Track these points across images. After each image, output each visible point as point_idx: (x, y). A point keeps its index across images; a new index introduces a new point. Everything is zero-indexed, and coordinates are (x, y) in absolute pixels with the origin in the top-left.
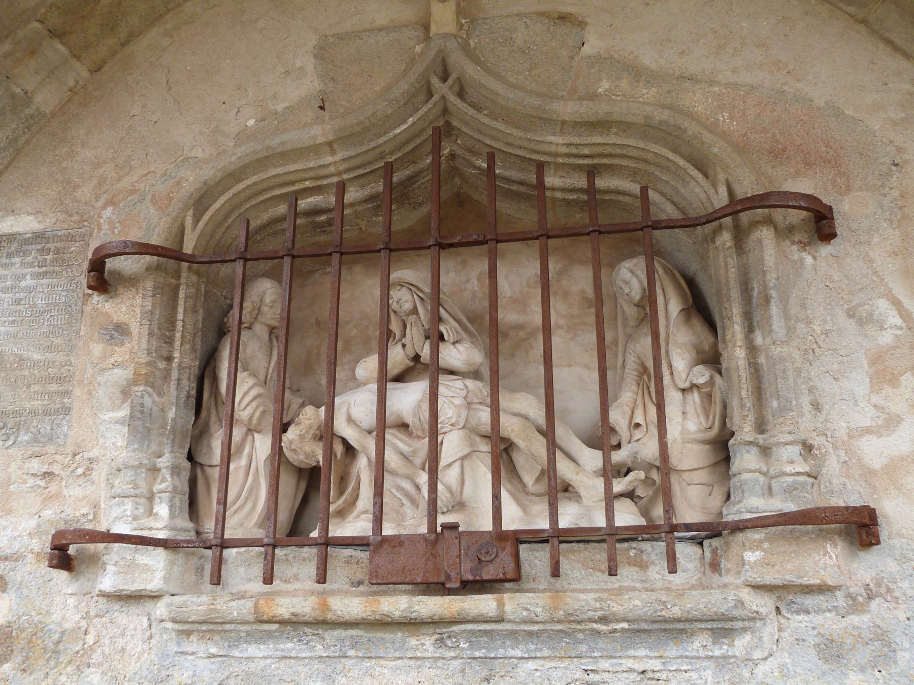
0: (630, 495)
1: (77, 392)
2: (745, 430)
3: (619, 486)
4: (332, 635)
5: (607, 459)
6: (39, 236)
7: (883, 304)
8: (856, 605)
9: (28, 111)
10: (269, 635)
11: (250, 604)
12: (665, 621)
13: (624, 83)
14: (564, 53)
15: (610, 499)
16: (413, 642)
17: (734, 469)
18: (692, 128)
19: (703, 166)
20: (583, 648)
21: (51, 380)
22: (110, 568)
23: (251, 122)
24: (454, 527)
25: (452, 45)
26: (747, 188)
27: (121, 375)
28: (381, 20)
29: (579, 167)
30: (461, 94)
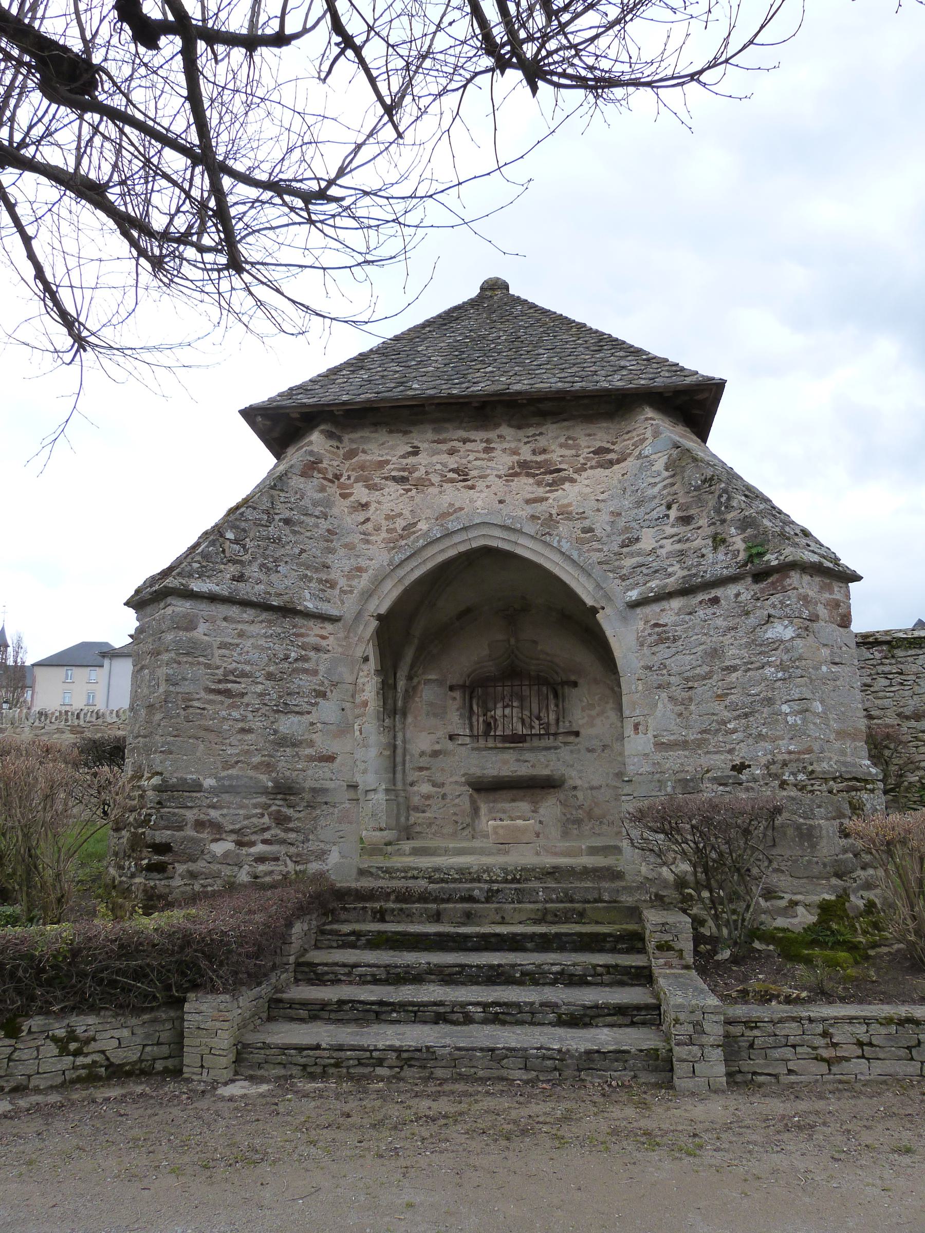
2: (561, 719)
6: (436, 680)
8: (576, 745)
19: (557, 673)
26: (564, 679)
27: (456, 707)
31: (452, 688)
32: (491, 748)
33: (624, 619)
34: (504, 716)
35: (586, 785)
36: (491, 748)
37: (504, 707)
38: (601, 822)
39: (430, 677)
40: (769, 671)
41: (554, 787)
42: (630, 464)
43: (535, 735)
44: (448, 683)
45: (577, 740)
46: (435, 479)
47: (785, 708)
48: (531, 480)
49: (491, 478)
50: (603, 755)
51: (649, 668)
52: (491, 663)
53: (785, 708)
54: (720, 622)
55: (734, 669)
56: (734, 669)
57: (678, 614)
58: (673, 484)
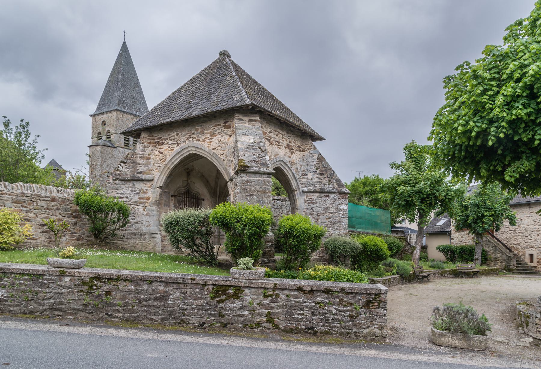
31: (172, 196)
33: (301, 195)
40: (340, 215)
42: (306, 153)
46: (274, 143)
47: (343, 224)
48: (289, 150)
49: (283, 147)
51: (308, 209)
53: (343, 224)
54: (329, 202)
55: (331, 213)
56: (331, 213)
57: (317, 197)
58: (318, 164)
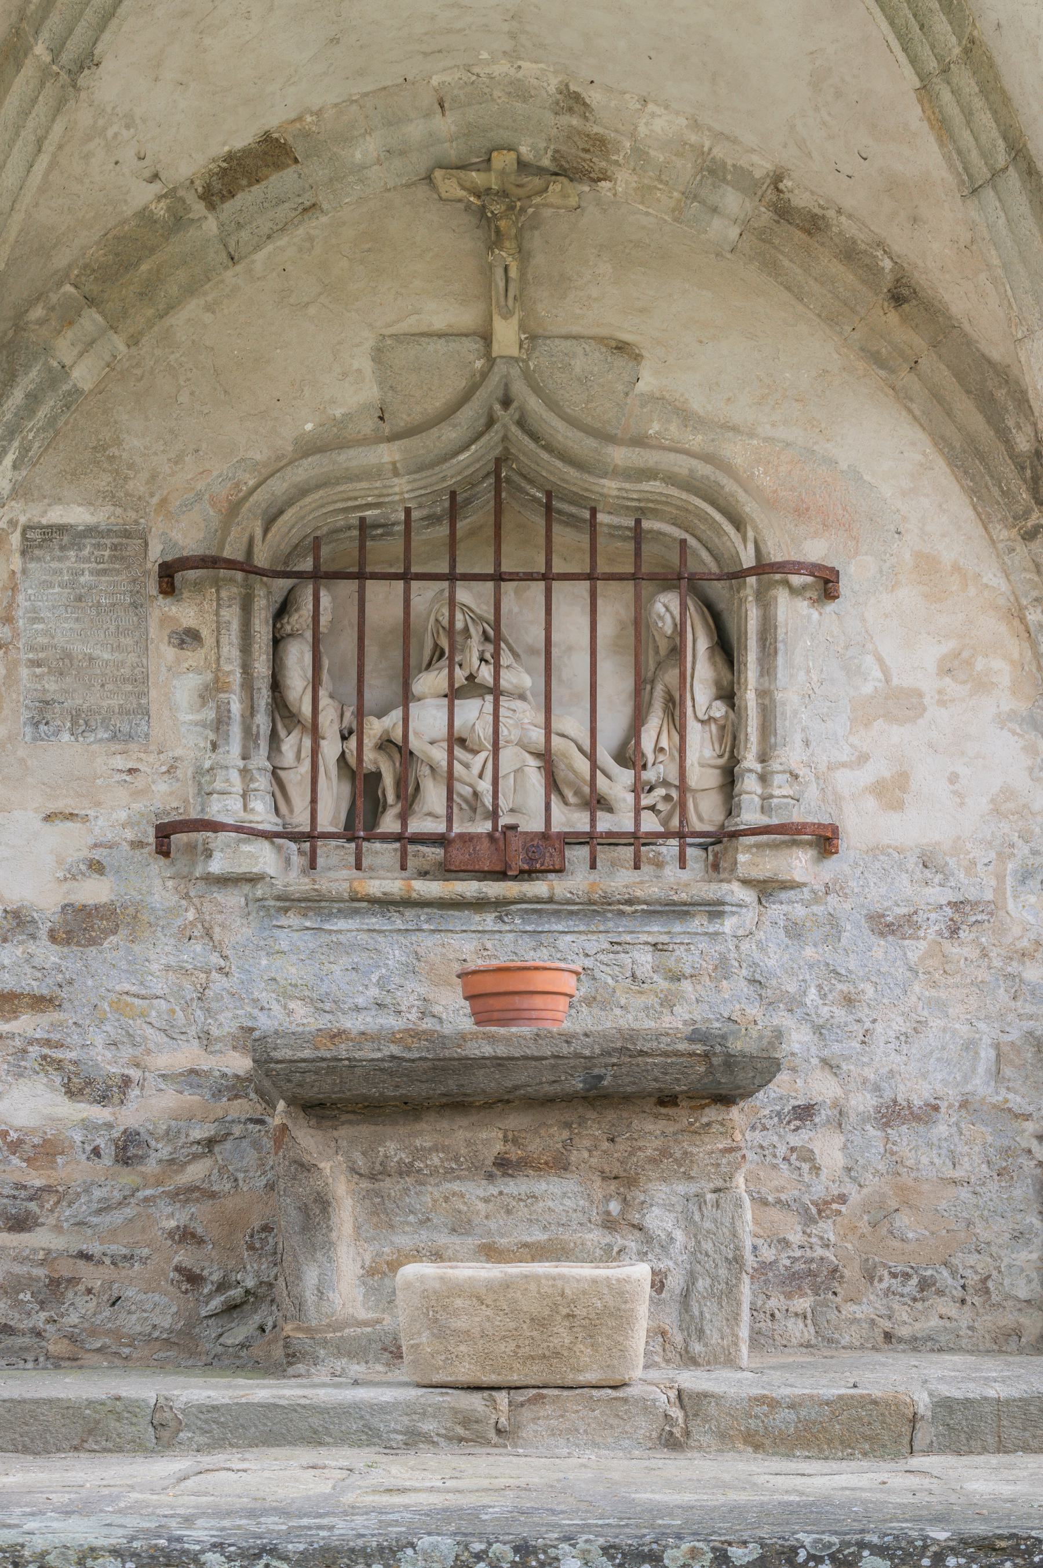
0: (652, 808)
1: (153, 693)
3: (646, 800)
4: (410, 913)
5: (637, 778)
6: (91, 531)
7: (869, 660)
9: (66, 387)
10: (356, 912)
11: (346, 885)
12: (674, 904)
13: (673, 428)
14: (620, 387)
15: (638, 810)
16: (477, 918)
17: (736, 790)
18: (729, 486)
20: (610, 925)
21: (125, 680)
22: (217, 855)
23: (309, 427)
24: (513, 828)
25: (515, 372)
28: (439, 324)
29: (628, 508)
30: (521, 423)
32: (385, 904)
34: (456, 741)
35: (862, 1102)
36: (385, 904)
37: (453, 694)
38: (925, 1285)
39: (56, 515)
41: (725, 1100)
43: (613, 839)
44: (156, 553)
45: (832, 868)
50: (953, 949)
52: (386, 454)
